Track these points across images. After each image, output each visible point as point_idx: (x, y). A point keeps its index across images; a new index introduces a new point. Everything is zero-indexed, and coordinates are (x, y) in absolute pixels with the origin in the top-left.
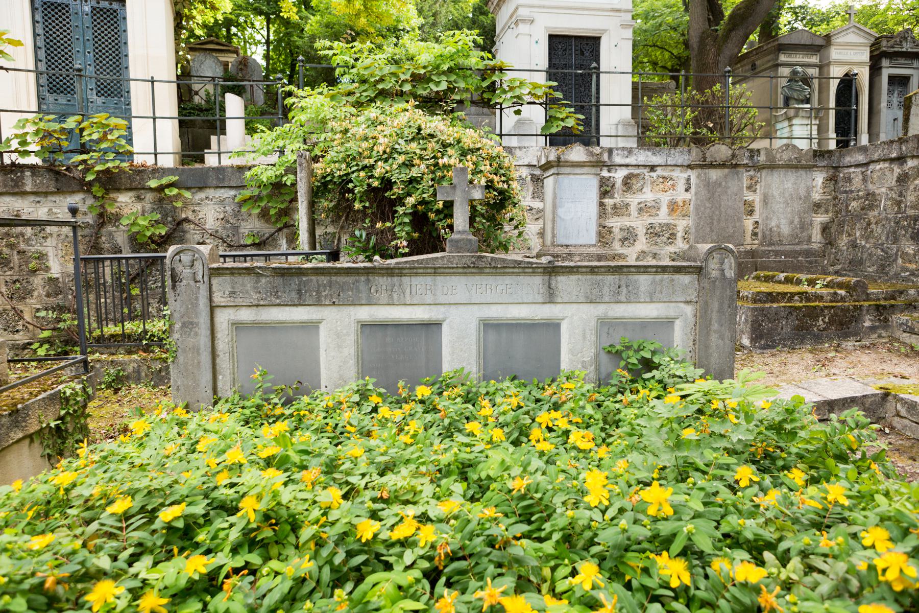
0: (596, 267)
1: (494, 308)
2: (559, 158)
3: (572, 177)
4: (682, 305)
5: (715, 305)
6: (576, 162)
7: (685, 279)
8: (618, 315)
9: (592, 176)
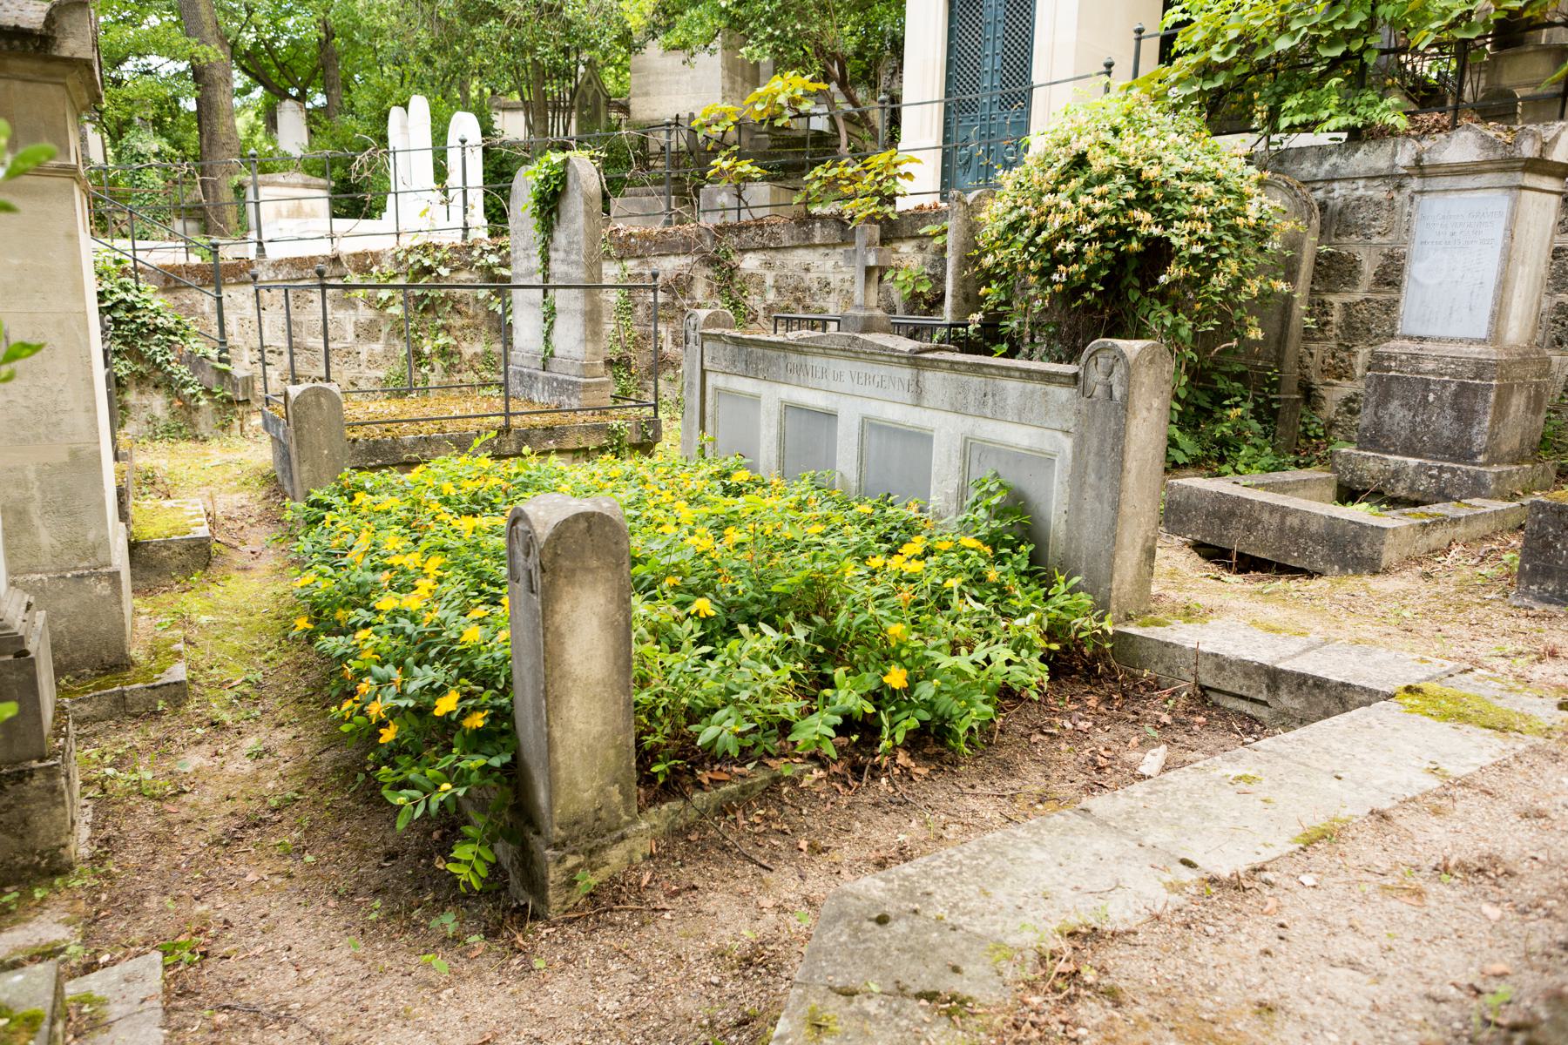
0: (958, 363)
1: (874, 404)
2: (1418, 160)
3: (1453, 196)
4: (1060, 435)
5: (1094, 442)
6: (1458, 164)
7: (1063, 394)
8: (985, 436)
9: (1500, 191)
